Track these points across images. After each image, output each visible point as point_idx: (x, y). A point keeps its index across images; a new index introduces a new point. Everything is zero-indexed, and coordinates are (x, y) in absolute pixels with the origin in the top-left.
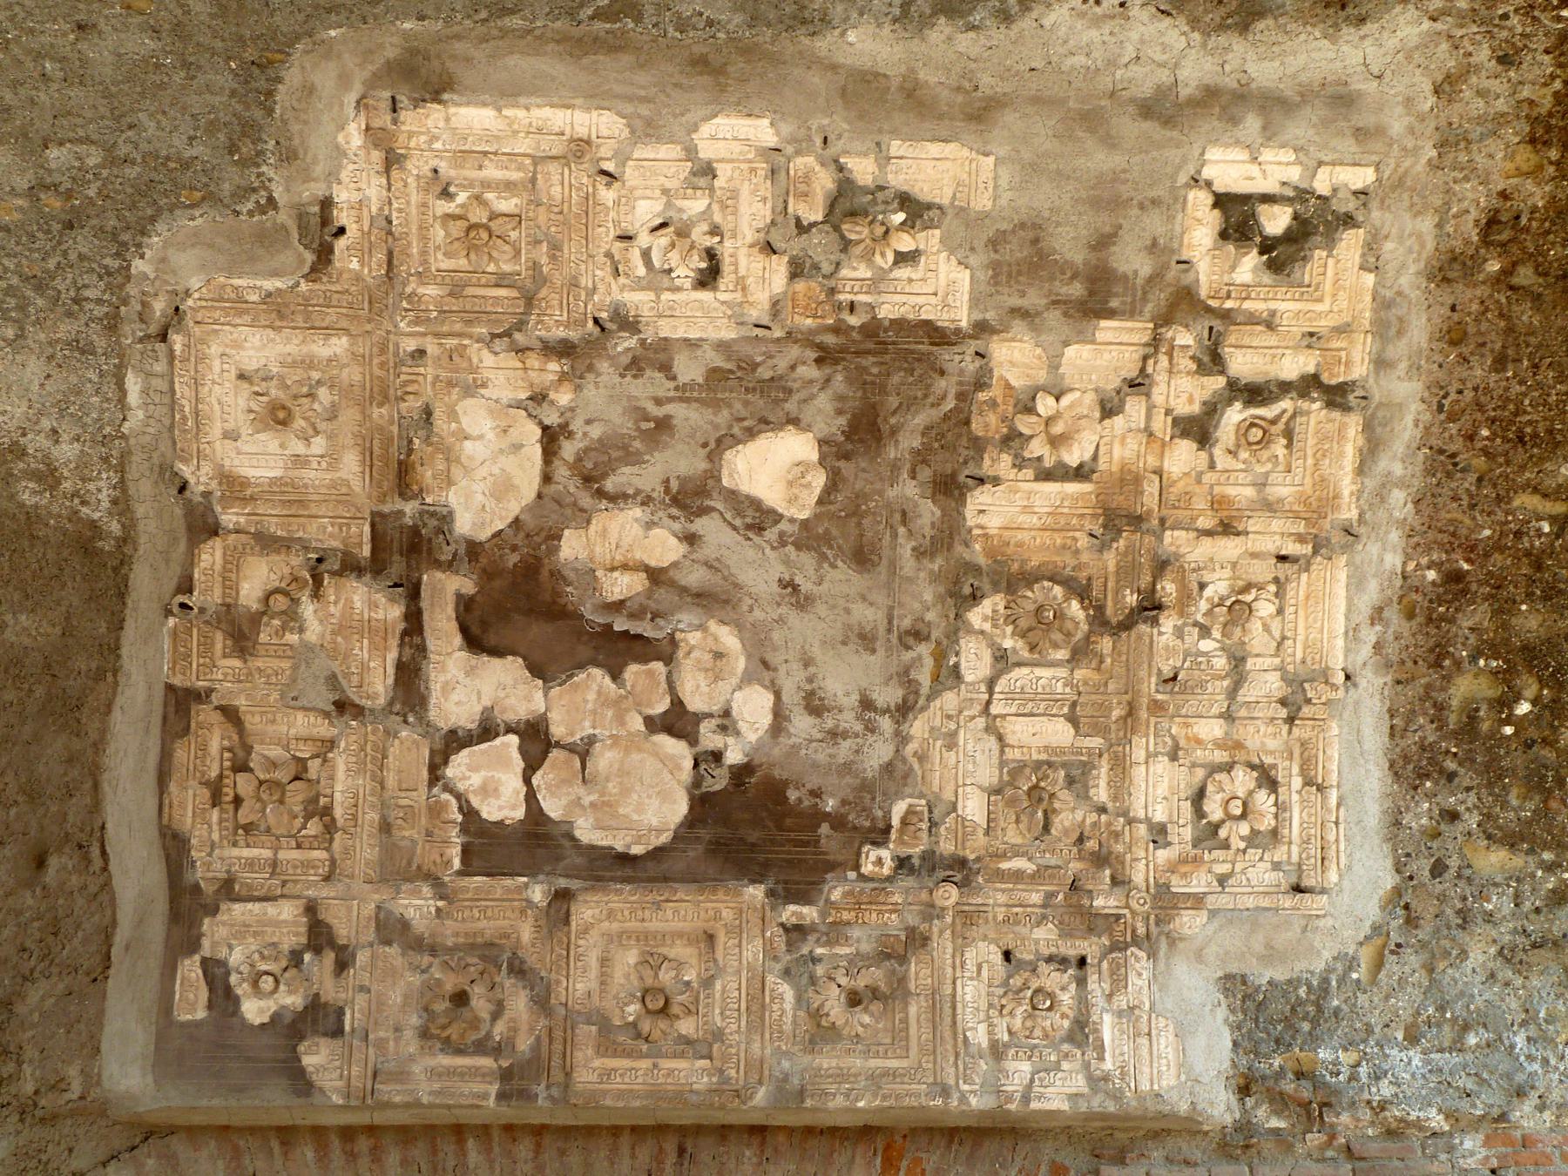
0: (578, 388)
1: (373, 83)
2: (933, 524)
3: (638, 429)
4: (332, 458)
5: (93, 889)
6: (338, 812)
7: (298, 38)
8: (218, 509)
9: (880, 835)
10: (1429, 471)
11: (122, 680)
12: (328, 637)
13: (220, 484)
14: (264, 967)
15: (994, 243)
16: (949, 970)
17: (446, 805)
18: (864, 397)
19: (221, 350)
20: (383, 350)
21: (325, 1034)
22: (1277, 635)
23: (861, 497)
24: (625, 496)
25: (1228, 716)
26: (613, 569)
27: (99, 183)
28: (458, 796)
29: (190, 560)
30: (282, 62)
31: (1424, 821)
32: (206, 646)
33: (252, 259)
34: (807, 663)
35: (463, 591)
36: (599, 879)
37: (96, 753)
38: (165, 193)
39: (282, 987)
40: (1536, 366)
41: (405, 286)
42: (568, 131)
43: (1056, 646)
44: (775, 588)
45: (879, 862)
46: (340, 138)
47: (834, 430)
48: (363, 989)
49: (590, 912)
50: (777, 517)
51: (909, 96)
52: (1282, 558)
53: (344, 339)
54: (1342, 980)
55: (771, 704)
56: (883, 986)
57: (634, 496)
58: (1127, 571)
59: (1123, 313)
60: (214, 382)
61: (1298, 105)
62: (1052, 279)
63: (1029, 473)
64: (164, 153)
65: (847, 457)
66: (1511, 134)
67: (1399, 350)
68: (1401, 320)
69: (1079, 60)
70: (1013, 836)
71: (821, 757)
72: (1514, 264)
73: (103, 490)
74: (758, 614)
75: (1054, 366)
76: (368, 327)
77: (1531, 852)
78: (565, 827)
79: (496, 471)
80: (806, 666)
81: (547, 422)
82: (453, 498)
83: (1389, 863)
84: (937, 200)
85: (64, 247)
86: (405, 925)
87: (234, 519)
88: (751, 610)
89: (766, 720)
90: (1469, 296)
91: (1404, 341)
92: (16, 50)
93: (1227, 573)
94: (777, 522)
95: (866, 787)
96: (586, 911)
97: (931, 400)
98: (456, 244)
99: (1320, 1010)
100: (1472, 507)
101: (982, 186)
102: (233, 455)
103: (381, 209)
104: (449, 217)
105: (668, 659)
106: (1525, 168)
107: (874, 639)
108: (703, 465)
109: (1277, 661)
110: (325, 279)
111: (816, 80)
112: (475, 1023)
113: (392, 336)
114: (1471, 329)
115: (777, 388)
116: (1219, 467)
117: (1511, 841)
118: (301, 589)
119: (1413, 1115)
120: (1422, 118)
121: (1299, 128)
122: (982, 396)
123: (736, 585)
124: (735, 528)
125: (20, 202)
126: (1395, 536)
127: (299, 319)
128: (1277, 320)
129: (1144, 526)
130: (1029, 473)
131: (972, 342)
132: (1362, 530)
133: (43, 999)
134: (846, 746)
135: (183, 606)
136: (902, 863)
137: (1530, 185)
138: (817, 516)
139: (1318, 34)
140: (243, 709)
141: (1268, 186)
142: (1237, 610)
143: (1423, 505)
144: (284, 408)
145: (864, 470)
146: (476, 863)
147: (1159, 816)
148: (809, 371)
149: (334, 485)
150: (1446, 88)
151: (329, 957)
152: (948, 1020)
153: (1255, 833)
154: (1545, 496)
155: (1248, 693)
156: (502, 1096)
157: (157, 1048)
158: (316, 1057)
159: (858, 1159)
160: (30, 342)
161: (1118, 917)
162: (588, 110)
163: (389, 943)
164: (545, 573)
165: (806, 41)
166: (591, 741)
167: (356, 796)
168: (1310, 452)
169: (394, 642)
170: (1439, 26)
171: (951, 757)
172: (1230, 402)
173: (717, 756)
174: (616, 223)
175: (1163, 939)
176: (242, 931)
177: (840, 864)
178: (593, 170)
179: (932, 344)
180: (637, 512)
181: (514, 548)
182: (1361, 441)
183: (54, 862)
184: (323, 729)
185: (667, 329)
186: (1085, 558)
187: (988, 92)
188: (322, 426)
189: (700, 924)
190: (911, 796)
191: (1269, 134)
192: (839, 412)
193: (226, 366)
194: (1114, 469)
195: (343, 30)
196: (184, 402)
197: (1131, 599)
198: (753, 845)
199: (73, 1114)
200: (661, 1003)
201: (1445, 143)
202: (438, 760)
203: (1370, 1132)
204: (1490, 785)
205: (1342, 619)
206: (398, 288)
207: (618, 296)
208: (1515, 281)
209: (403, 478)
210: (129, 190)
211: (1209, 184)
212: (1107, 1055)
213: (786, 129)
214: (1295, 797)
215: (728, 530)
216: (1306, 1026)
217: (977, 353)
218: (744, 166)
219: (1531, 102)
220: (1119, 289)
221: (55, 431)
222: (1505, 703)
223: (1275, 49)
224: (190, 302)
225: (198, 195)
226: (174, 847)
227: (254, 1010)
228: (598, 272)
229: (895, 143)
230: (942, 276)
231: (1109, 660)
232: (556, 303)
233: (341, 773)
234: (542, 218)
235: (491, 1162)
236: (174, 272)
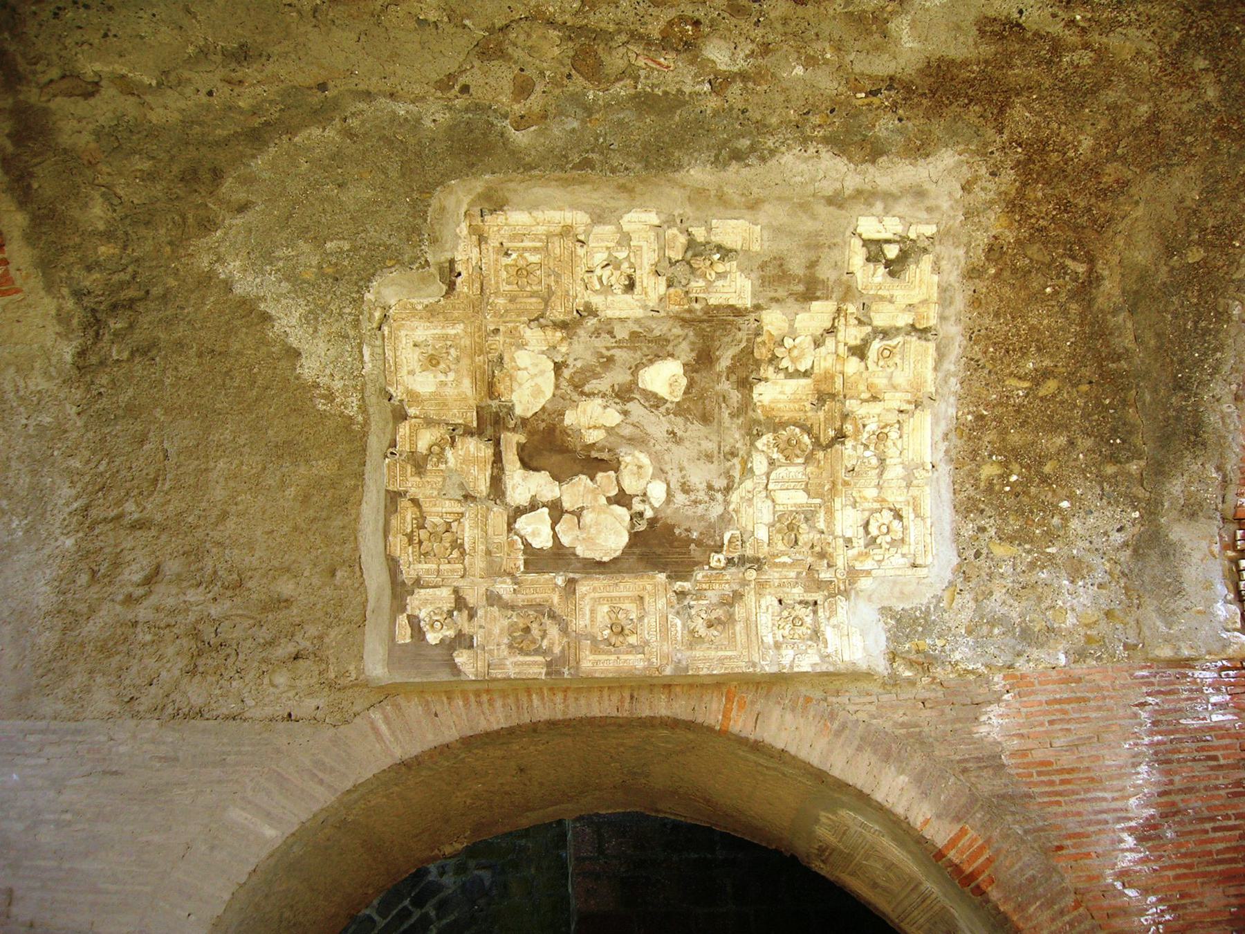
0: (571, 343)
1: (472, 204)
4: (458, 382)
5: (356, 585)
6: (466, 546)
9: (719, 549)
14: (436, 618)
15: (762, 267)
16: (754, 610)
20: (480, 329)
23: (704, 390)
24: (594, 394)
26: (589, 428)
28: (521, 537)
29: (395, 431)
32: (403, 468)
33: (419, 290)
36: (588, 573)
43: (798, 457)
45: (719, 560)
46: (458, 231)
48: (481, 627)
54: (935, 607)
57: (598, 394)
58: (829, 420)
61: (900, 197)
63: (782, 375)
65: (696, 371)
67: (951, 312)
69: (798, 179)
70: (781, 546)
71: (690, 513)
73: (354, 401)
74: (658, 447)
75: (791, 326)
76: (473, 319)
77: (1020, 545)
78: (572, 550)
80: (681, 471)
82: (515, 398)
83: (955, 553)
86: (500, 597)
89: (663, 496)
90: (981, 286)
91: (953, 308)
93: (876, 419)
94: (665, 403)
95: (711, 526)
96: (582, 588)
99: (926, 621)
100: (987, 385)
104: (506, 266)
105: (617, 470)
107: (712, 457)
108: (630, 378)
109: (900, 460)
111: (676, 193)
112: (534, 641)
115: (662, 341)
117: (1011, 539)
118: (446, 443)
119: (970, 668)
120: (957, 201)
121: (901, 207)
122: (759, 339)
123: (646, 434)
124: (645, 407)
126: (952, 399)
127: (441, 317)
130: (782, 375)
132: (937, 398)
133: (336, 636)
134: (700, 509)
135: (392, 453)
136: (730, 561)
137: (1007, 232)
140: (421, 500)
141: (889, 236)
142: (881, 437)
143: (964, 384)
146: (531, 567)
147: (848, 535)
148: (677, 331)
151: (466, 612)
152: (754, 633)
154: (1020, 378)
155: (886, 476)
156: (547, 674)
158: (462, 658)
159: (715, 699)
161: (831, 582)
163: (492, 606)
164: (558, 432)
165: (671, 175)
166: (582, 508)
167: (474, 538)
169: (489, 467)
170: (962, 158)
171: (750, 511)
172: (875, 338)
173: (641, 514)
176: (426, 602)
180: (599, 401)
181: (543, 421)
182: (935, 355)
183: (339, 574)
184: (458, 508)
185: (610, 314)
186: (809, 414)
188: (453, 367)
189: (637, 593)
191: (887, 211)
194: (822, 372)
197: (832, 433)
199: (353, 686)
201: (968, 215)
202: (511, 520)
203: (951, 676)
204: (1000, 514)
206: (485, 300)
207: (587, 299)
209: (491, 390)
211: (860, 235)
213: (663, 217)
214: (911, 523)
216: (920, 629)
219: (1006, 194)
220: (820, 287)
222: (1004, 477)
225: (392, 262)
226: (393, 565)
229: (714, 222)
230: (738, 284)
233: (467, 526)
235: (544, 704)
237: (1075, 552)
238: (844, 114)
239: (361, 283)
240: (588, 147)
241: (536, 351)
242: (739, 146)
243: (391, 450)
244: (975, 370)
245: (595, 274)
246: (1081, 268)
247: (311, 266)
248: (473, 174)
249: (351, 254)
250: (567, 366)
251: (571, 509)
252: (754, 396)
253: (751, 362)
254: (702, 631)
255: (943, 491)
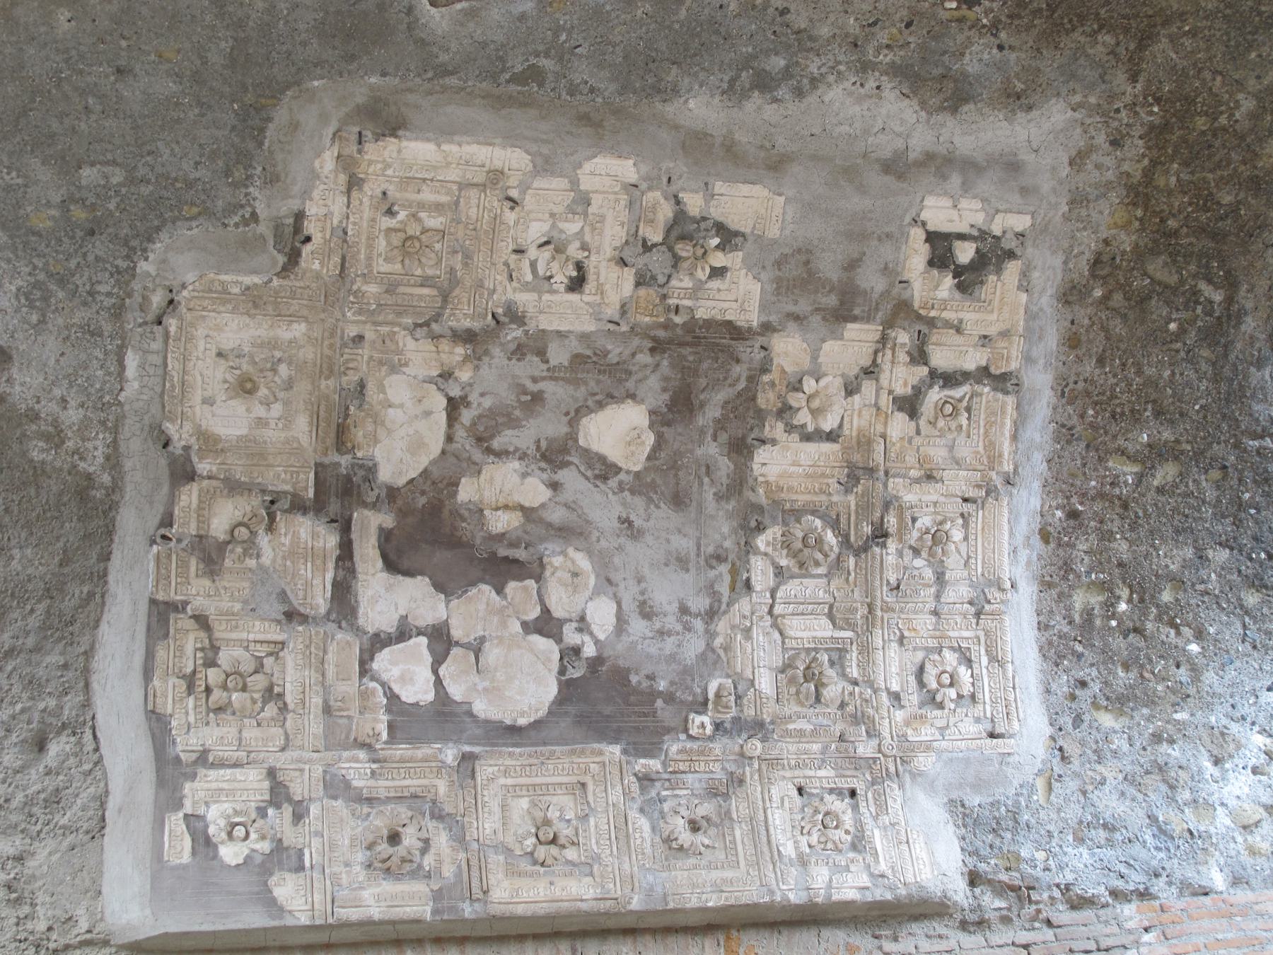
0: (477, 368)
1: (345, 122)
2: (728, 475)
3: (519, 401)
4: (287, 420)
5: (87, 767)
6: (289, 699)
7: (288, 88)
8: (195, 459)
9: (702, 705)
10: (1057, 440)
11: (109, 600)
12: (279, 561)
13: (198, 439)
14: (237, 820)
15: (779, 264)
17: (374, 691)
18: (683, 379)
19: (206, 332)
20: (332, 335)
21: (290, 870)
22: (965, 556)
23: (678, 454)
24: (507, 453)
25: (935, 613)
26: (497, 509)
27: (118, 199)
28: (383, 684)
29: (172, 500)
30: (275, 105)
31: (1065, 689)
32: (183, 565)
34: (640, 581)
35: (384, 525)
37: (87, 660)
38: (171, 209)
39: (253, 836)
40: (1124, 365)
41: (352, 283)
42: (488, 164)
43: (817, 564)
44: (616, 524)
45: (703, 726)
46: (317, 164)
47: (660, 403)
49: (490, 770)
50: (618, 470)
51: (728, 151)
52: (965, 500)
53: (303, 325)
55: (614, 611)
56: (715, 818)
58: (865, 507)
59: (862, 319)
60: (198, 359)
62: (816, 292)
63: (795, 436)
64: (173, 175)
65: (668, 424)
66: (1114, 197)
67: (1038, 351)
68: (1041, 328)
69: (845, 129)
71: (653, 650)
72: (1111, 292)
73: (98, 448)
74: (603, 543)
75: (815, 358)
76: (322, 316)
78: (465, 707)
79: (411, 432)
80: (639, 582)
81: (452, 394)
82: (379, 453)
83: (1046, 720)
84: (742, 230)
85: (84, 250)
86: (347, 784)
87: (208, 467)
88: (598, 541)
90: (1083, 315)
92: (66, 87)
95: (686, 671)
96: (485, 770)
97: (729, 381)
98: (396, 251)
99: (1016, 822)
101: (774, 219)
102: (209, 417)
103: (341, 222)
105: (539, 578)
106: (1120, 223)
108: (565, 429)
110: (292, 277)
113: (341, 323)
114: (1084, 338)
116: (923, 433)
121: (985, 185)
122: (766, 378)
123: (587, 522)
124: (587, 478)
125: (53, 212)
126: (1037, 485)
127: (270, 308)
128: (964, 326)
129: (875, 476)
130: (795, 436)
131: (760, 338)
133: (50, 854)
134: (670, 642)
135: (164, 537)
136: (718, 726)
137: (1123, 236)
138: (645, 468)
139: (1001, 117)
141: (963, 228)
142: (938, 538)
144: (250, 380)
145: (680, 434)
147: (895, 687)
148: (644, 358)
149: (287, 441)
150: (1077, 161)
151: (287, 810)
152: (764, 839)
153: (960, 696)
155: (950, 595)
156: (435, 912)
157: (152, 888)
158: (286, 889)
160: (50, 326)
161: (874, 759)
162: (504, 147)
163: (335, 798)
164: (446, 513)
165: (659, 106)
166: (482, 640)
168: (982, 423)
169: (331, 565)
170: (1077, 115)
172: (931, 386)
173: (576, 651)
174: (515, 239)
175: (907, 775)
176: (216, 795)
177: (673, 729)
178: (501, 196)
179: (732, 339)
180: (516, 464)
181: (423, 493)
183: (55, 749)
185: (547, 323)
186: (835, 498)
187: (782, 150)
189: (574, 779)
190: (721, 677)
191: (966, 188)
192: (664, 390)
193: (208, 346)
194: (854, 434)
195: (324, 81)
196: (174, 373)
197: (867, 529)
198: (608, 716)
200: (551, 836)
201: (1072, 202)
202: (366, 656)
205: (1006, 545)
206: (348, 286)
207: (510, 295)
208: (1111, 304)
209: (341, 438)
210: (142, 205)
211: (924, 224)
212: (881, 859)
213: (644, 169)
214: (984, 671)
215: (582, 479)
216: (1008, 835)
217: (762, 347)
218: (612, 197)
219: (1128, 175)
220: (860, 300)
221: (64, 400)
222: (1110, 605)
223: (974, 126)
224: (185, 293)
225: (195, 210)
227: (231, 853)
228: (498, 277)
229: (719, 184)
231: (853, 574)
232: (465, 300)
234: (460, 234)
236: (174, 271)
237: (1213, 719)
238: (925, 32)
239: (135, 243)
240: (541, 48)
241: (421, 377)
242: (768, 68)
243: (163, 531)
244: (1069, 442)
245: (526, 255)
246: (1218, 297)
247: (49, 204)
248: (349, 73)
249: (124, 190)
250: (468, 405)
251: (466, 640)
252: (755, 467)
253: (751, 413)
254: (685, 837)
255: (1025, 625)
